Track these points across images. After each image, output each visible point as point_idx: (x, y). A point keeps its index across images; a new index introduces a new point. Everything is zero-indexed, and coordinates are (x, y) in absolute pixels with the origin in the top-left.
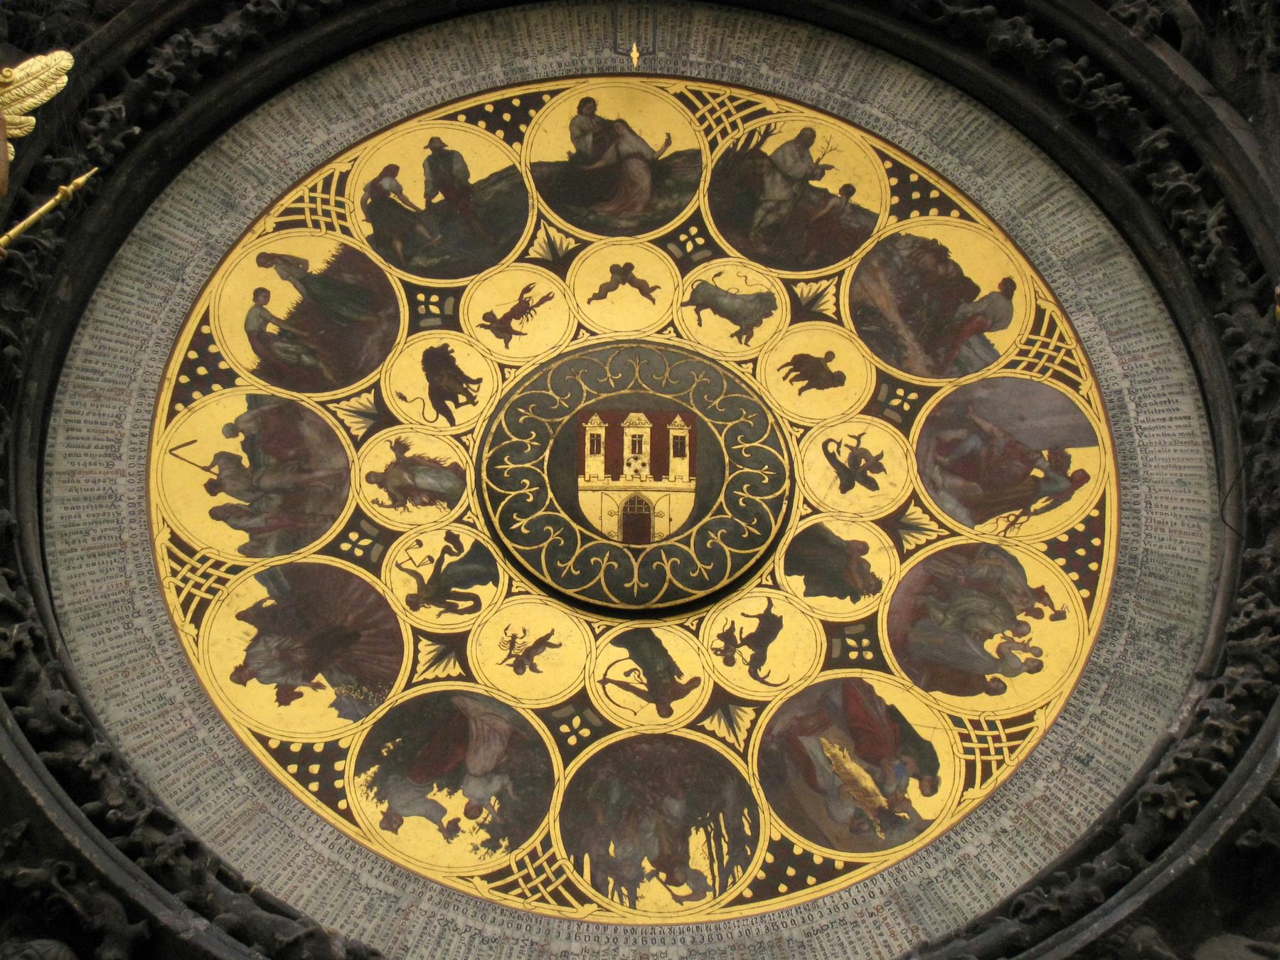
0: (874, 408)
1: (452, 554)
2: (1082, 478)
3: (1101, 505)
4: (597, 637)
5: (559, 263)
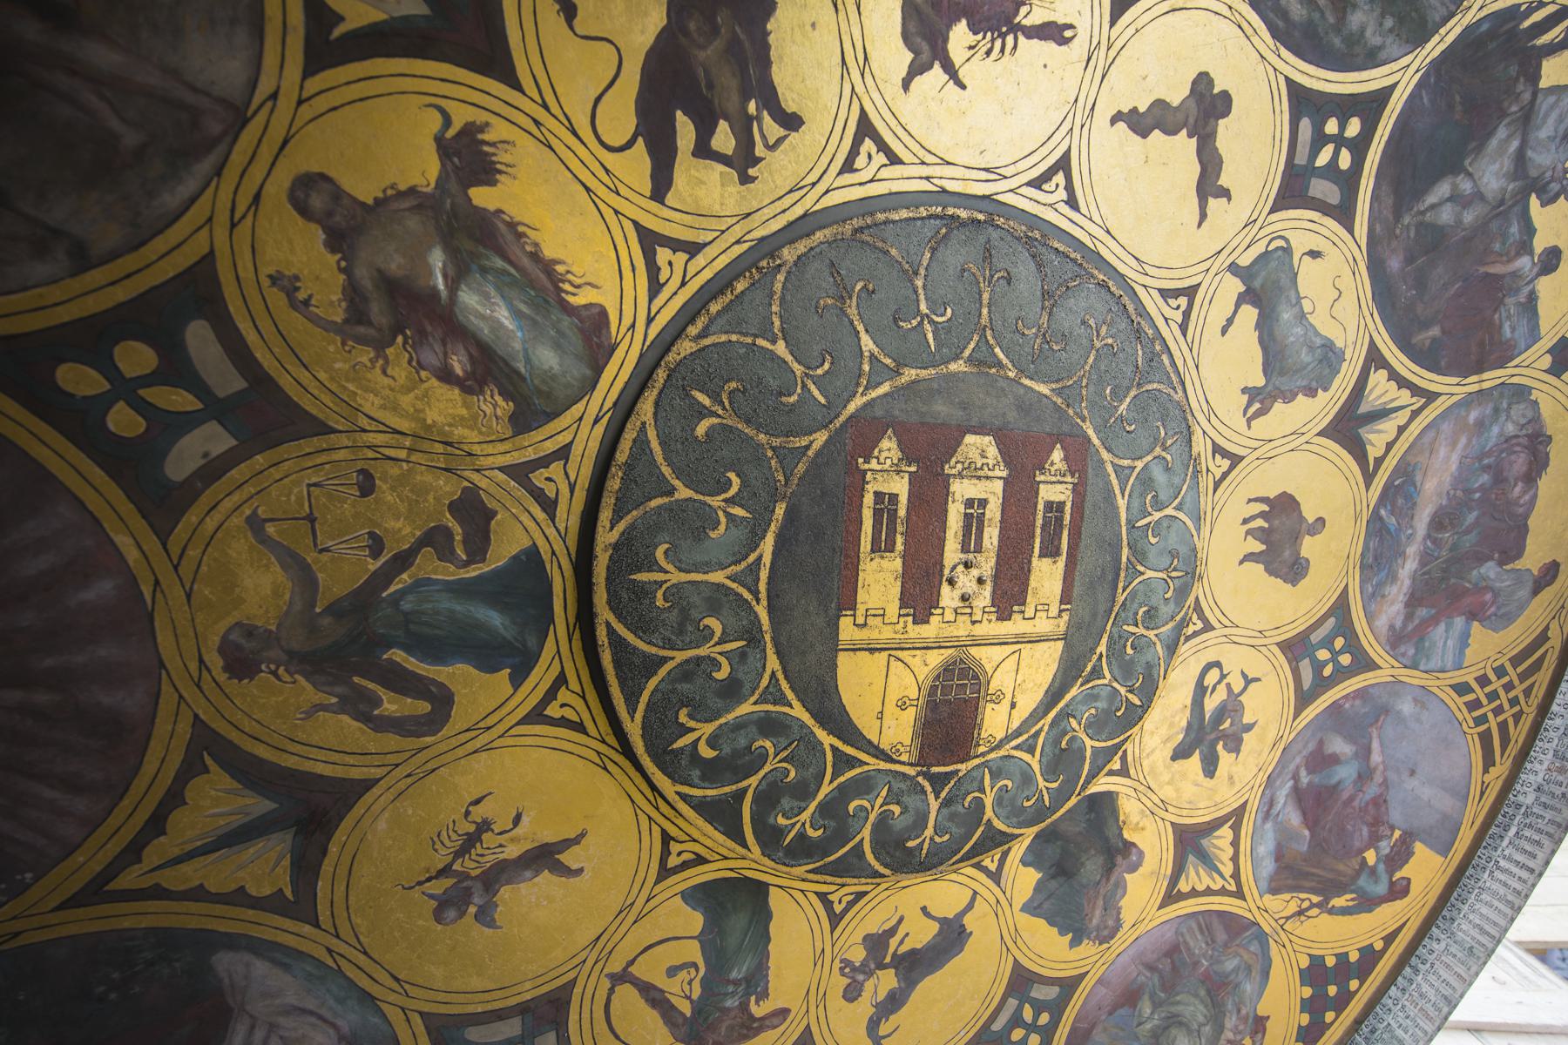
0: (1296, 648)
1: (446, 554)
3: (1389, 939)
4: (665, 872)
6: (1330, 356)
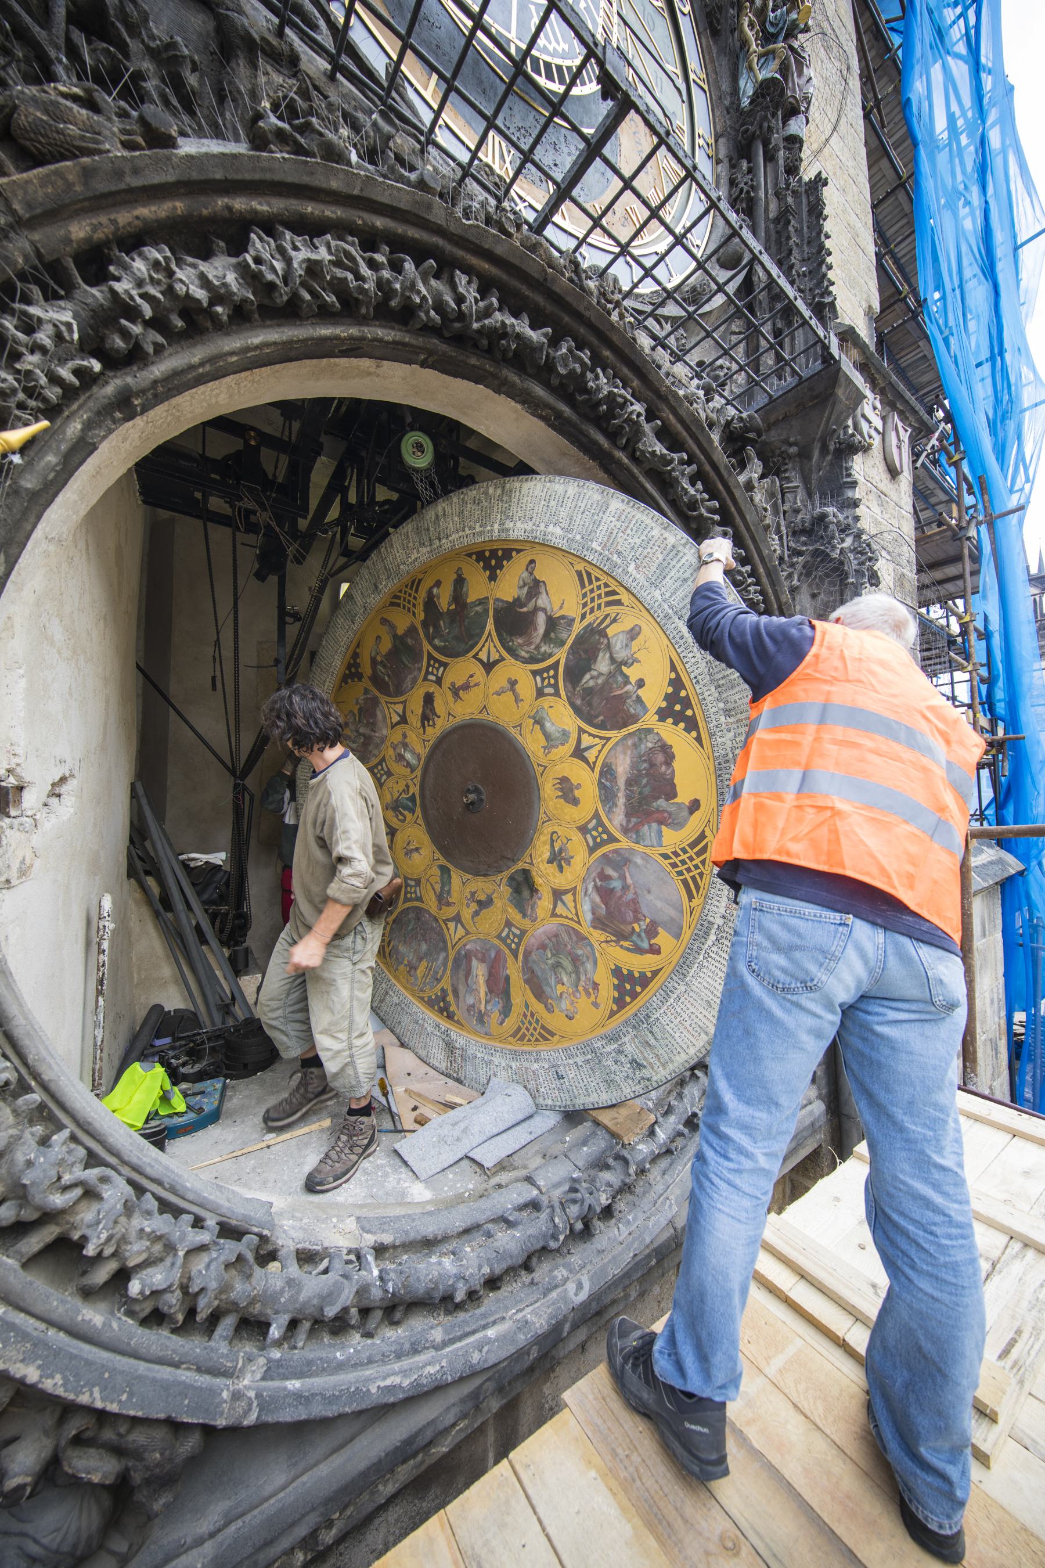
2: (655, 950)
3: (655, 973)
5: (489, 667)
6: (565, 734)
